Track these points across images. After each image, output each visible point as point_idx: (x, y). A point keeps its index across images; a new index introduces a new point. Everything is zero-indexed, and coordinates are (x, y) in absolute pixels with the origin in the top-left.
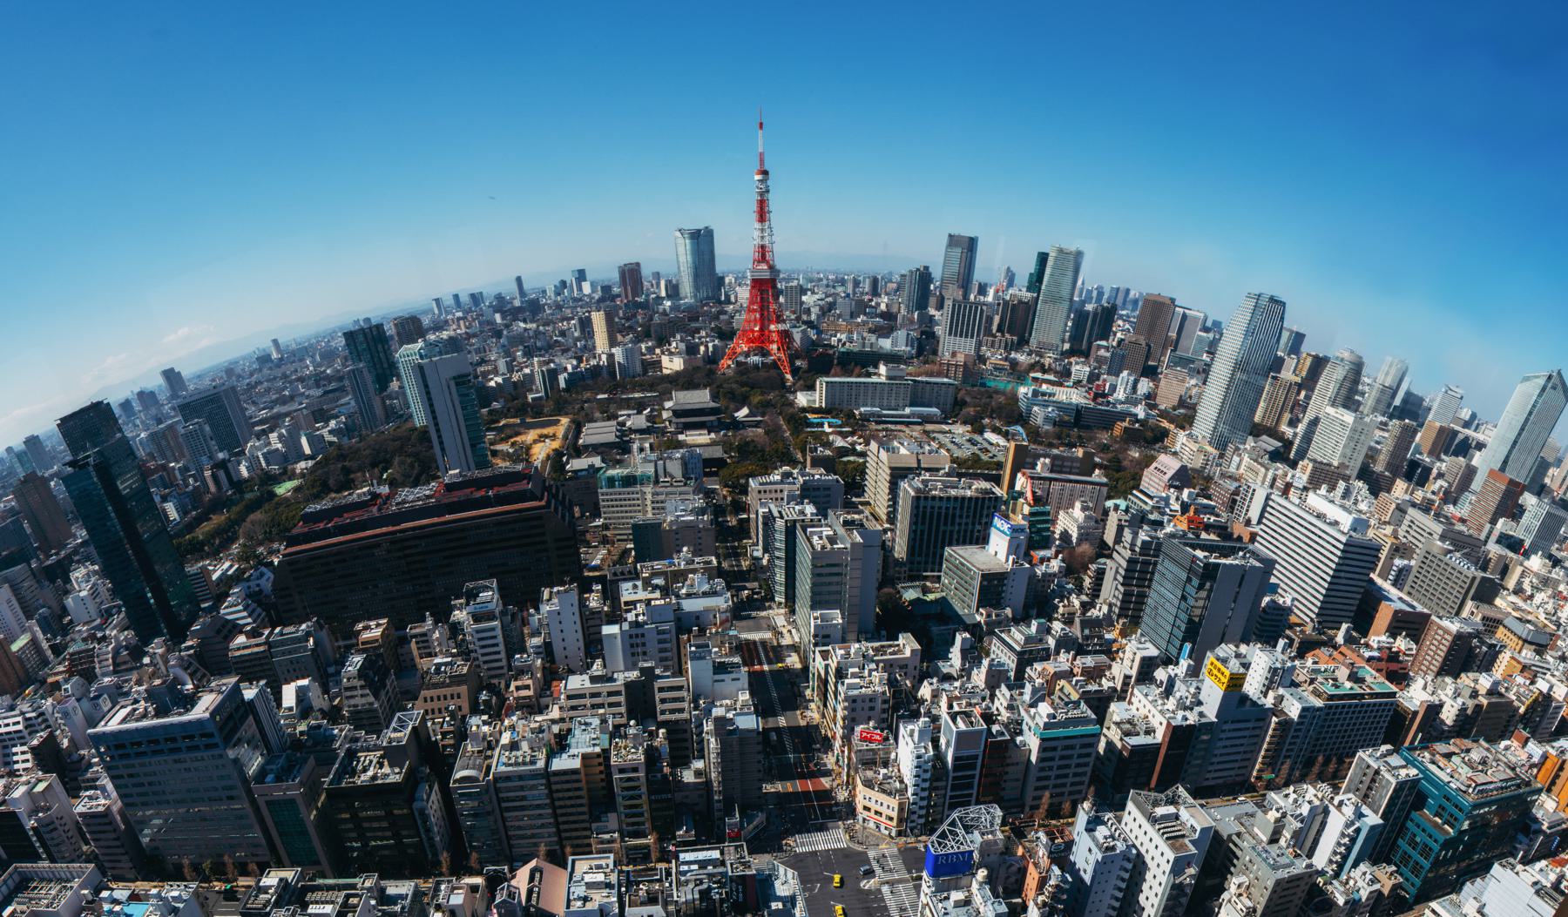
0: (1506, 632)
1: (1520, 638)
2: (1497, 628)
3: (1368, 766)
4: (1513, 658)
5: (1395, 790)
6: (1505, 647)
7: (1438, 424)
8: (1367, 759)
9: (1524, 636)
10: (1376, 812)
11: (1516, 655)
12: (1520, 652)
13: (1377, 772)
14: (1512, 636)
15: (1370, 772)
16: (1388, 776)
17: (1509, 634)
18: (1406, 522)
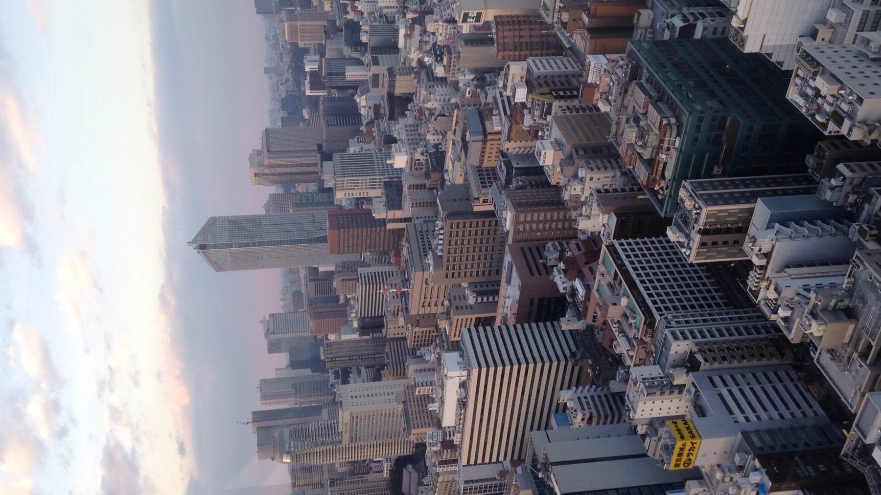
0: (486, 158)
1: (485, 142)
2: (487, 170)
3: (703, 244)
4: (509, 139)
5: (715, 203)
6: (502, 152)
7: (311, 323)
8: (694, 251)
9: (481, 138)
10: (751, 212)
11: (504, 136)
12: (499, 133)
13: (703, 232)
14: (488, 150)
15: (709, 239)
16: (702, 219)
17: (487, 155)
18: (427, 310)
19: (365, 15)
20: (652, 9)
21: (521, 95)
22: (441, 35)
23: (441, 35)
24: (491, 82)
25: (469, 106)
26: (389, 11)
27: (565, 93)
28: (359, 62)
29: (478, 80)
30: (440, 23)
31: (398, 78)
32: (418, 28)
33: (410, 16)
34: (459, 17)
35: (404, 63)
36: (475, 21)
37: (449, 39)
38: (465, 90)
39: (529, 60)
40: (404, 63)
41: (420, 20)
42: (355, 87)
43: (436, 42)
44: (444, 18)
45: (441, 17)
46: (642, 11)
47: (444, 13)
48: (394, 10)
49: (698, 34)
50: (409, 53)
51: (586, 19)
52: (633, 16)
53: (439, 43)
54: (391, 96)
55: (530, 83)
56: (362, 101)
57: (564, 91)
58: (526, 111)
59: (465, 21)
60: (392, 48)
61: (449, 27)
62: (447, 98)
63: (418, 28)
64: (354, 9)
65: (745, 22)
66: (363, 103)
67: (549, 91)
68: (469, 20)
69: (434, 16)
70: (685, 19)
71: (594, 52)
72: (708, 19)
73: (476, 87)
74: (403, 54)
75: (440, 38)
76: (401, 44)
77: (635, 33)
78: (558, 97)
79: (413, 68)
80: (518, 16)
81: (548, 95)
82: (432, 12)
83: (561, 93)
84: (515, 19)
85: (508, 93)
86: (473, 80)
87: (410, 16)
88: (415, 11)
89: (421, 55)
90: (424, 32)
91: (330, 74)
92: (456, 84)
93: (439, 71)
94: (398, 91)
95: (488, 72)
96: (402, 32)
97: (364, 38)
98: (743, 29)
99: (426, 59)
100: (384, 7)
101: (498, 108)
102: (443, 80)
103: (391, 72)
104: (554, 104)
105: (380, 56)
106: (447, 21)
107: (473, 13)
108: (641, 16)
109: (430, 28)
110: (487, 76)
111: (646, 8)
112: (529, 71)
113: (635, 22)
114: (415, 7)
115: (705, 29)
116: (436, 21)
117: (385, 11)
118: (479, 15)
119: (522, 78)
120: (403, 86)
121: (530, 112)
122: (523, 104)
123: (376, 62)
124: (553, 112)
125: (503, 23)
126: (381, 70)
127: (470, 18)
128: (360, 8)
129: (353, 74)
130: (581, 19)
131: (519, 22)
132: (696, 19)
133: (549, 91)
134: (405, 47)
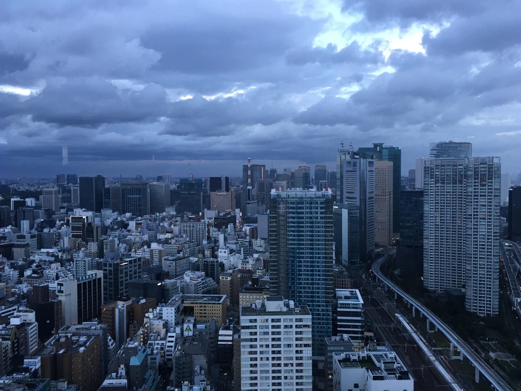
19: (59, 231)
20: (67, 388)
21: (15, 322)
22: (49, 272)
23: (49, 272)
24: (22, 303)
25: (7, 291)
26: (62, 243)
27: (16, 347)
28: (31, 228)
29: (23, 295)
30: (56, 271)
31: (23, 249)
32: (53, 259)
33: (60, 254)
34: (61, 281)
35: (32, 252)
36: (58, 290)
37: (47, 277)
38: (16, 288)
39: (36, 323)
40: (32, 252)
41: (57, 260)
42: (17, 225)
43: (45, 270)
44: (59, 273)
45: (59, 271)
46: (66, 383)
47: (62, 272)
48: (62, 245)
50: (38, 254)
51: (61, 352)
52: (63, 378)
53: (44, 271)
54: (13, 246)
55: (24, 325)
56: (8, 229)
57: (17, 346)
58: (4, 325)
59: (58, 284)
60: (41, 246)
62: (11, 278)
64: (62, 225)
66: (7, 230)
67: (17, 337)
68: (59, 287)
69: (59, 268)
71: (42, 360)
73: (19, 294)
74: (37, 252)
75: (47, 271)
76: (43, 250)
77: (54, 381)
78: (13, 343)
79: (29, 258)
80: (61, 314)
81: (14, 338)
82: (62, 266)
83: (16, 345)
84: (59, 312)
85: (16, 314)
86: (23, 292)
87: (60, 254)
88: (62, 257)
89: (37, 261)
90: (51, 262)
91: (24, 212)
92: (20, 282)
93: (28, 273)
94: (15, 250)
95: (27, 300)
96: (51, 251)
97: (46, 230)
99: (35, 265)
100: (64, 241)
101: (6, 308)
102: (21, 275)
103: (28, 245)
104: (9, 342)
105: (36, 239)
106: (57, 274)
107: (63, 288)
108: (63, 383)
109: (53, 266)
110: (26, 300)
111: (68, 384)
112: (30, 324)
113: (60, 380)
114: (64, 257)
116: (57, 269)
117: (62, 241)
118: (61, 292)
119: (25, 321)
120: (17, 252)
121: (3, 328)
122: (9, 323)
123: (32, 237)
124: (4, 342)
125: (58, 306)
126: (28, 240)
127: (60, 287)
128: (62, 227)
129: (25, 224)
130: (61, 349)
131: (58, 315)
133: (17, 337)
134: (41, 253)
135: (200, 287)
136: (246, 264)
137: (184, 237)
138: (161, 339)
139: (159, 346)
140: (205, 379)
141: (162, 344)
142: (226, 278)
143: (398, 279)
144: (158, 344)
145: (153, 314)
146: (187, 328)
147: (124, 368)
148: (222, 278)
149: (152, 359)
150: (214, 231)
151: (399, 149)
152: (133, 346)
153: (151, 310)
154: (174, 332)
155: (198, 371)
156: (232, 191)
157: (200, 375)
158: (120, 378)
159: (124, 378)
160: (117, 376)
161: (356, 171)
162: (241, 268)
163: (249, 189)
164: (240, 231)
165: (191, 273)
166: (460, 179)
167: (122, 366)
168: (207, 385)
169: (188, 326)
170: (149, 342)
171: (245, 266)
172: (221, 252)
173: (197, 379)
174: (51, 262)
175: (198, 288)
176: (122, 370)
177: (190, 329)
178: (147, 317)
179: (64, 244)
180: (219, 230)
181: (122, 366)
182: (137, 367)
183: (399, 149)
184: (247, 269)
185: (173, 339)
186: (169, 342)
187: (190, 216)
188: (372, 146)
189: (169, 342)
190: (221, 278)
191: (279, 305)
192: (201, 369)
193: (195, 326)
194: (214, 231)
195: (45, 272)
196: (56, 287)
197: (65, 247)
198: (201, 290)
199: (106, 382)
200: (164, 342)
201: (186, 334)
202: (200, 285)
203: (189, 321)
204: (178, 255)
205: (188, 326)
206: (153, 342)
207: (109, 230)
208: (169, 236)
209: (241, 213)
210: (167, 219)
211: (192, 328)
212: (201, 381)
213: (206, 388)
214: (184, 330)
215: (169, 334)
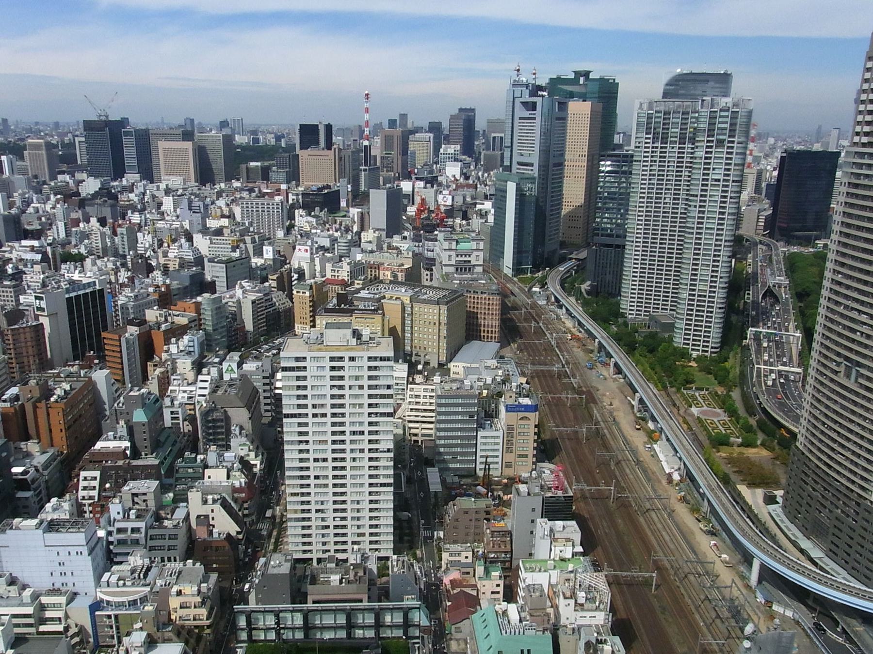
23: (32, 278)
30: (42, 276)
32: (39, 257)
36: (37, 307)
43: (26, 274)
45: (47, 277)
49: (21, 494)
53: (24, 276)
61: (39, 284)
63: (39, 257)
65: (17, 528)
68: (37, 301)
70: (33, 481)
72: (37, 500)
76: (25, 243)
89: (14, 260)
98: (11, 528)
99: (11, 266)
100: (57, 227)
115: (27, 498)
117: (54, 227)
125: (38, 331)
132: (35, 490)
135: (263, 306)
136: (338, 271)
137: (247, 225)
138: (189, 384)
139: (186, 395)
140: (248, 443)
141: (191, 391)
142: (303, 293)
143: (586, 296)
144: (185, 392)
145: (178, 347)
146: (227, 370)
147: (125, 426)
148: (298, 292)
149: (172, 413)
150: (301, 216)
151: (616, 81)
152: (137, 394)
153: (173, 340)
154: (209, 374)
155: (237, 432)
156: (335, 149)
157: (239, 437)
158: (120, 439)
159: (125, 440)
160: (115, 438)
161: (534, 119)
162: (330, 278)
163: (366, 146)
164: (345, 216)
165: (248, 284)
166: (691, 135)
167: (122, 423)
168: (250, 450)
169: (230, 366)
170: (170, 388)
171: (336, 274)
172: (300, 250)
173: (234, 442)
174: (34, 263)
175: (259, 308)
176: (122, 428)
177: (232, 370)
178: (167, 351)
179: (58, 233)
180: (310, 215)
181: (122, 423)
182: (144, 425)
183: (616, 81)
184: (340, 278)
185: (206, 385)
186: (201, 388)
187: (265, 191)
188: (572, 76)
189: (201, 388)
190: (294, 292)
191: (345, 336)
192: (241, 428)
193: (240, 365)
194: (301, 216)
195: (26, 277)
196: (34, 301)
197: (61, 237)
198: (263, 310)
199: (99, 445)
200: (192, 388)
201: (227, 377)
202: (262, 303)
203: (232, 360)
204: (233, 254)
205: (230, 366)
206: (177, 388)
207: (129, 212)
208: (225, 222)
209: (349, 186)
210: (224, 195)
211: (235, 369)
212: (240, 445)
213: (248, 455)
214: (224, 370)
215: (200, 377)
